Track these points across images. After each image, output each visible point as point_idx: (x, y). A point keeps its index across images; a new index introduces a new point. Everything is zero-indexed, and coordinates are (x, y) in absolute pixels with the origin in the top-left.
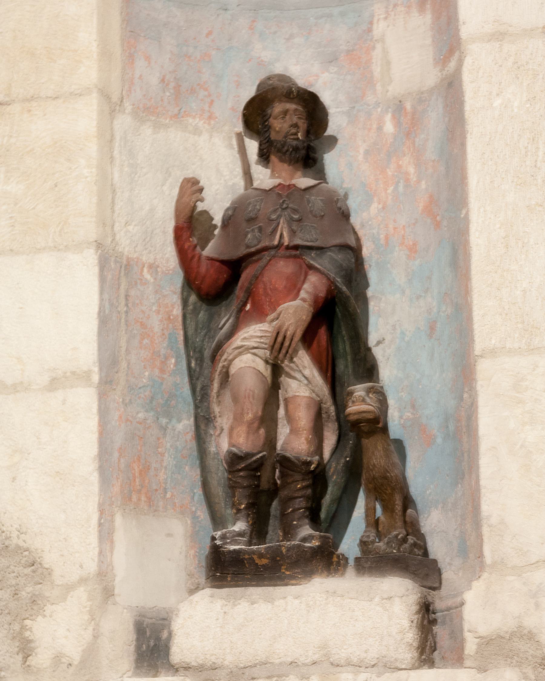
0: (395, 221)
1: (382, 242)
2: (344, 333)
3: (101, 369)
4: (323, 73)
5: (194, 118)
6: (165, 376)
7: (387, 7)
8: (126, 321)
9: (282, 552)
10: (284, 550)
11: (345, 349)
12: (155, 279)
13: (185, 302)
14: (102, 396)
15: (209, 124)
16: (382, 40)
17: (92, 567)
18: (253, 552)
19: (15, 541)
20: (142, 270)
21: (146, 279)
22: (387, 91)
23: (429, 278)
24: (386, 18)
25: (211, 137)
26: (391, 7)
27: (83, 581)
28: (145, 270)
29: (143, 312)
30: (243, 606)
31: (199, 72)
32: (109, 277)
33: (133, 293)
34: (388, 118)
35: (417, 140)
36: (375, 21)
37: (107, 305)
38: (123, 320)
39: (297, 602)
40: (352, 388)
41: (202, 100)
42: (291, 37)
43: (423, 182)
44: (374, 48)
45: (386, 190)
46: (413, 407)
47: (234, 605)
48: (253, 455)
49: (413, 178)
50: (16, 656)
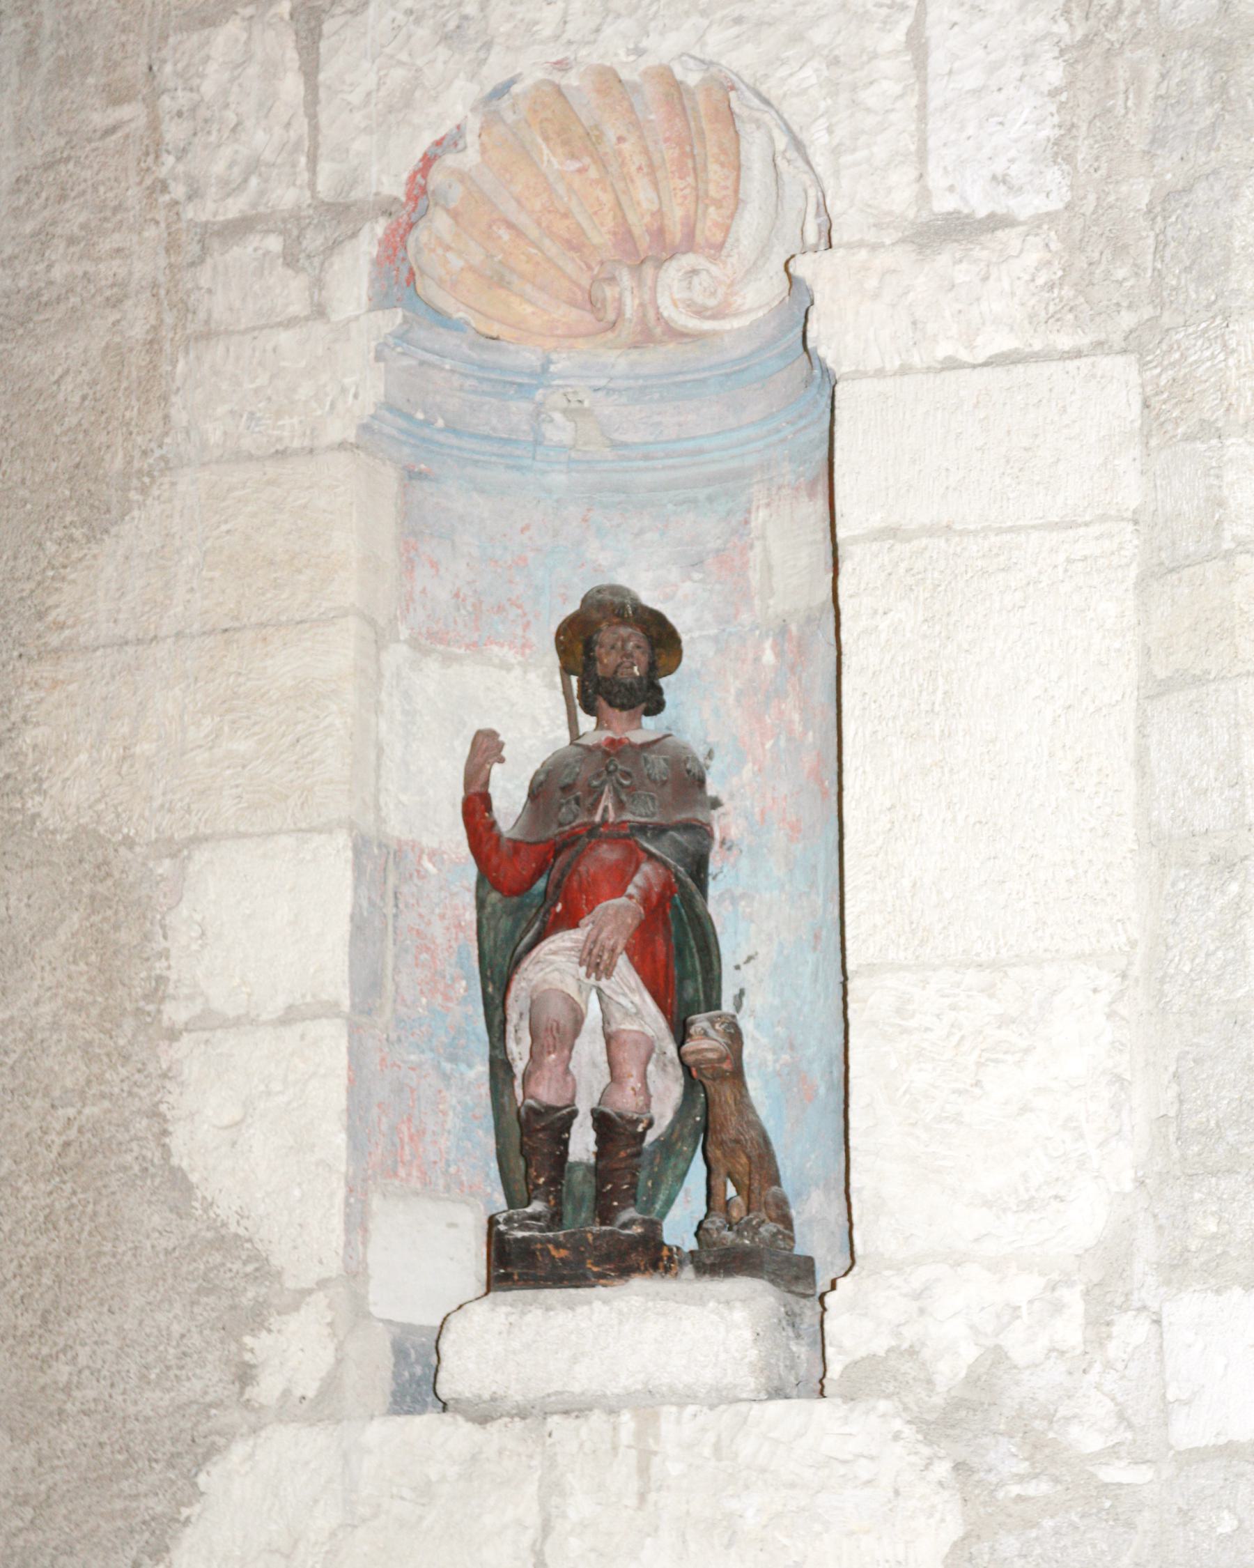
0: (774, 789)
1: (757, 817)
2: (692, 943)
3: (353, 993)
4: (683, 581)
5: (502, 646)
6: (450, 1005)
7: (769, 489)
8: (395, 928)
9: (587, 1240)
10: (590, 1237)
11: (693, 966)
12: (440, 870)
13: (481, 904)
14: (354, 1030)
15: (523, 654)
16: (763, 537)
17: (334, 1267)
18: (549, 1240)
19: (233, 1228)
20: (420, 858)
21: (426, 871)
23: (814, 867)
24: (768, 505)
25: (525, 672)
27: (322, 1284)
28: (425, 858)
29: (421, 916)
30: (535, 1316)
31: (511, 582)
32: (370, 867)
33: (405, 889)
34: (768, 644)
35: (804, 675)
36: (754, 509)
37: (365, 903)
38: (390, 928)
39: (606, 1309)
40: (693, 1017)
41: (513, 621)
43: (811, 734)
44: (752, 547)
45: (763, 745)
46: (792, 1047)
47: (523, 1313)
48: (559, 1109)
49: (798, 728)
50: (231, 1386)
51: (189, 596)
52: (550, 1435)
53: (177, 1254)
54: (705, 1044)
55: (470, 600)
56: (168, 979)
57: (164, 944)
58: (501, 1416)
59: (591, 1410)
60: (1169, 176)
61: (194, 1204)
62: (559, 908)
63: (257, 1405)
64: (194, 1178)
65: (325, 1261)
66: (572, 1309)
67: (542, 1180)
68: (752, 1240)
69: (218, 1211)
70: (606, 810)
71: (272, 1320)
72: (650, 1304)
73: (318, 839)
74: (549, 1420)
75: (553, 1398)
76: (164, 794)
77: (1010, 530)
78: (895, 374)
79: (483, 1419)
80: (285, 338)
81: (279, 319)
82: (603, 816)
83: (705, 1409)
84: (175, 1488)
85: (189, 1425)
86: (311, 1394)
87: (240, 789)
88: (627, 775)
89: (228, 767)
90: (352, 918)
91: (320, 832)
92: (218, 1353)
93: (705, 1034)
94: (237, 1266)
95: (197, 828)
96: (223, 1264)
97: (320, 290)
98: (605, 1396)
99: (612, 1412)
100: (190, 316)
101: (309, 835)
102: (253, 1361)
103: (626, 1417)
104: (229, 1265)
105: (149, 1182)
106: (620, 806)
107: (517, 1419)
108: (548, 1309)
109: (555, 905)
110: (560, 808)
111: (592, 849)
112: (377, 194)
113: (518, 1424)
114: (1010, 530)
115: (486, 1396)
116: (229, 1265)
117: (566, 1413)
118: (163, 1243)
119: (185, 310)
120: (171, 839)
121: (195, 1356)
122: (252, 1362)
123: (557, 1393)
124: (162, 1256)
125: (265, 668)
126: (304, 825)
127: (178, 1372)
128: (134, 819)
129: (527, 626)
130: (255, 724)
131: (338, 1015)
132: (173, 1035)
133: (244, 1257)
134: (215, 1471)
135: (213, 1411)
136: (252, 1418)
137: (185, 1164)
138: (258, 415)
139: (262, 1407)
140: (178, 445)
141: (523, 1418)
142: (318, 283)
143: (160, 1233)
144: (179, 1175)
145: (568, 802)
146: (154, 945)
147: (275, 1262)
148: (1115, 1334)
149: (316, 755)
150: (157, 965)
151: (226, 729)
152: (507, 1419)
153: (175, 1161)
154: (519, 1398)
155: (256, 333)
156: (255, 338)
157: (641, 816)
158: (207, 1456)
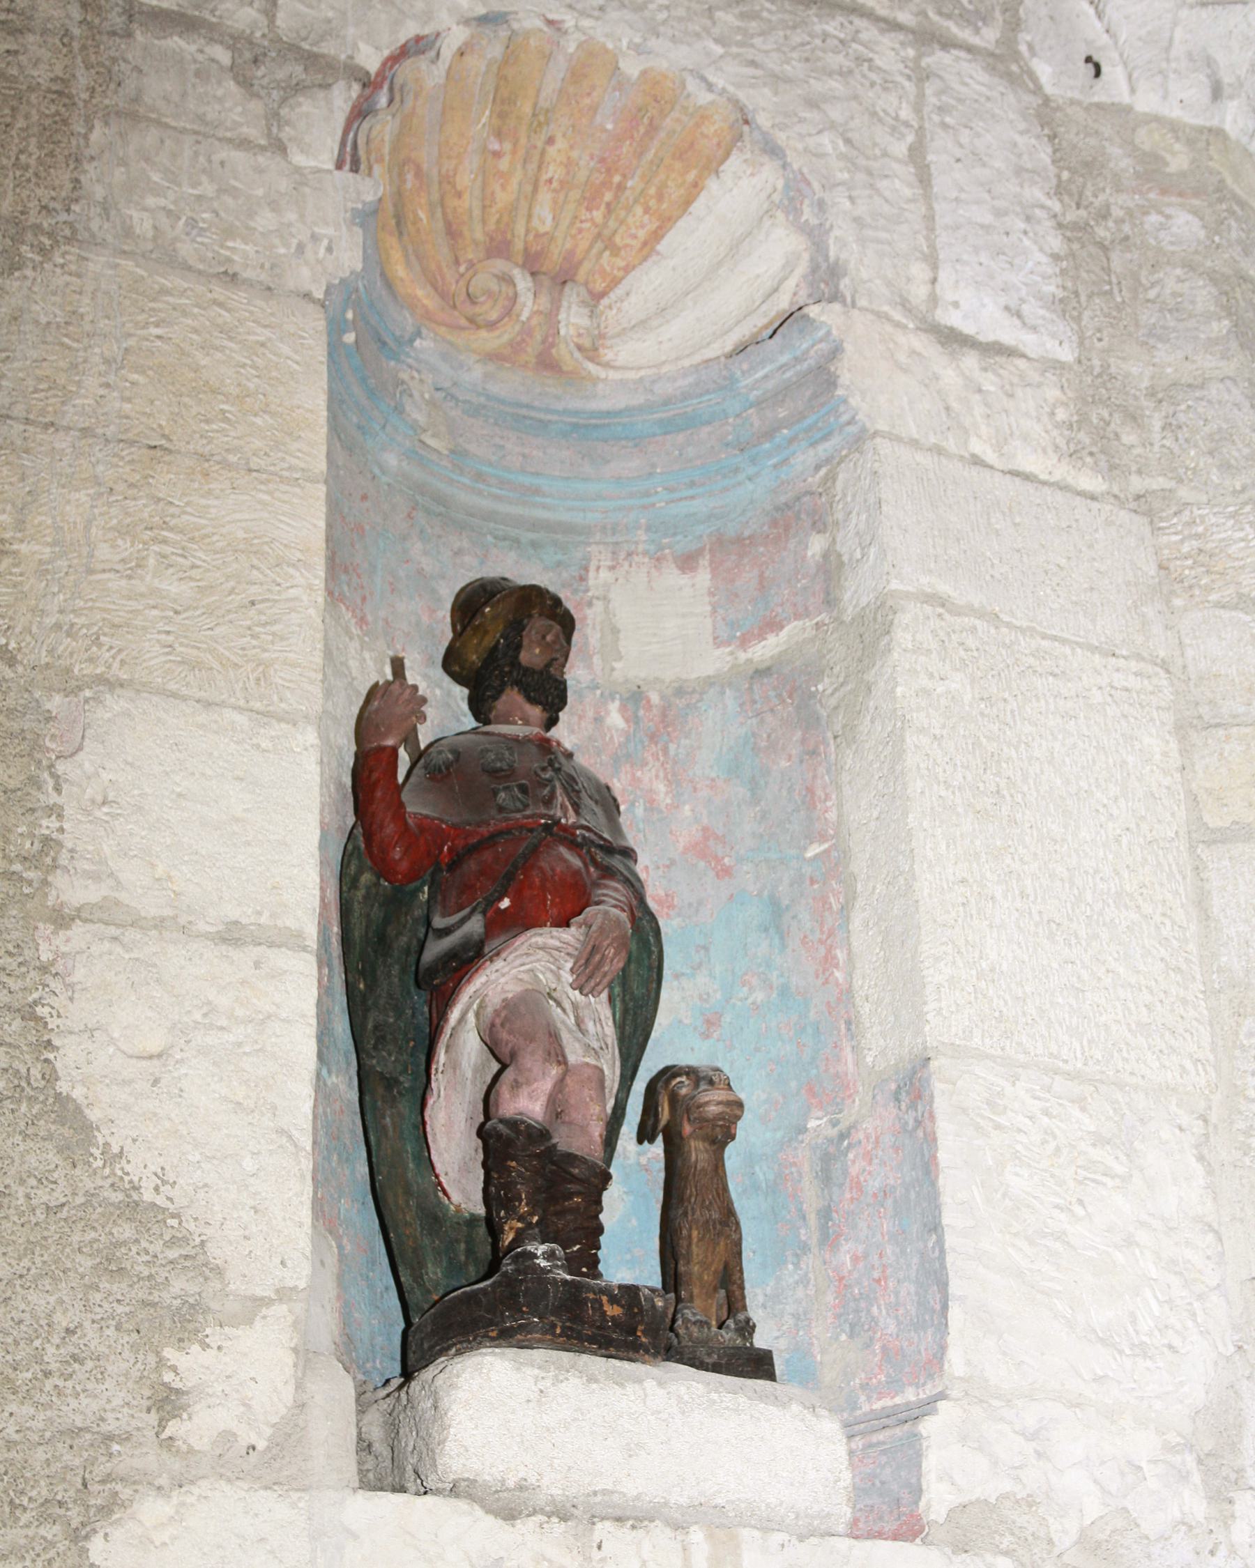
19: (148, 1196)
22: (613, 669)
26: (622, 555)
27: (283, 1294)
30: (573, 1386)
39: (661, 1392)
42: (458, 553)
47: (557, 1381)
50: (144, 1415)
51: (102, 392)
52: (599, 1547)
53: (64, 1213)
56: (60, 844)
57: (54, 798)
58: (534, 1513)
59: (652, 1521)
60: (1169, 370)
61: (93, 1150)
62: (505, 903)
63: (184, 1448)
64: (93, 1115)
65: (289, 1264)
66: (622, 1385)
67: (536, 1219)
69: (128, 1168)
71: (208, 1331)
72: (714, 1396)
73: (278, 728)
74: (599, 1526)
75: (599, 1498)
76: (61, 612)
77: (1055, 638)
78: (930, 449)
79: (509, 1515)
80: (238, 157)
81: (228, 135)
83: (794, 1540)
84: (52, 1553)
85: (77, 1462)
86: (261, 1445)
87: (171, 638)
89: (154, 607)
91: (280, 720)
92: (124, 1365)
94: (157, 1247)
95: (109, 667)
96: (137, 1241)
97: (279, 127)
98: (666, 1504)
99: (678, 1526)
100: (112, 86)
101: (265, 720)
102: (177, 1385)
103: (697, 1535)
104: (144, 1244)
105: (24, 1107)
107: (555, 1519)
109: (500, 899)
111: (548, 846)
112: (351, 57)
113: (557, 1527)
114: (1055, 638)
115: (511, 1483)
116: (144, 1244)
117: (619, 1519)
118: (42, 1196)
119: (108, 76)
120: (68, 670)
121: (90, 1364)
122: (175, 1385)
123: (605, 1492)
124: (40, 1216)
125: (208, 506)
126: (257, 705)
127: (61, 1383)
128: (17, 630)
130: (194, 567)
131: (305, 949)
132: (62, 919)
133: (167, 1237)
134: (117, 1534)
135: (116, 1447)
136: (176, 1465)
137: (78, 1093)
138: (201, 225)
139: (191, 1451)
140: (89, 219)
141: (564, 1518)
142: (274, 117)
143: (40, 1181)
144: (71, 1106)
146: (41, 797)
147: (216, 1253)
148: (1237, 1514)
149: (276, 628)
150: (45, 823)
151: (152, 561)
152: (541, 1518)
153: (63, 1087)
154: (556, 1491)
155: (200, 138)
156: (198, 142)
158: (106, 1510)
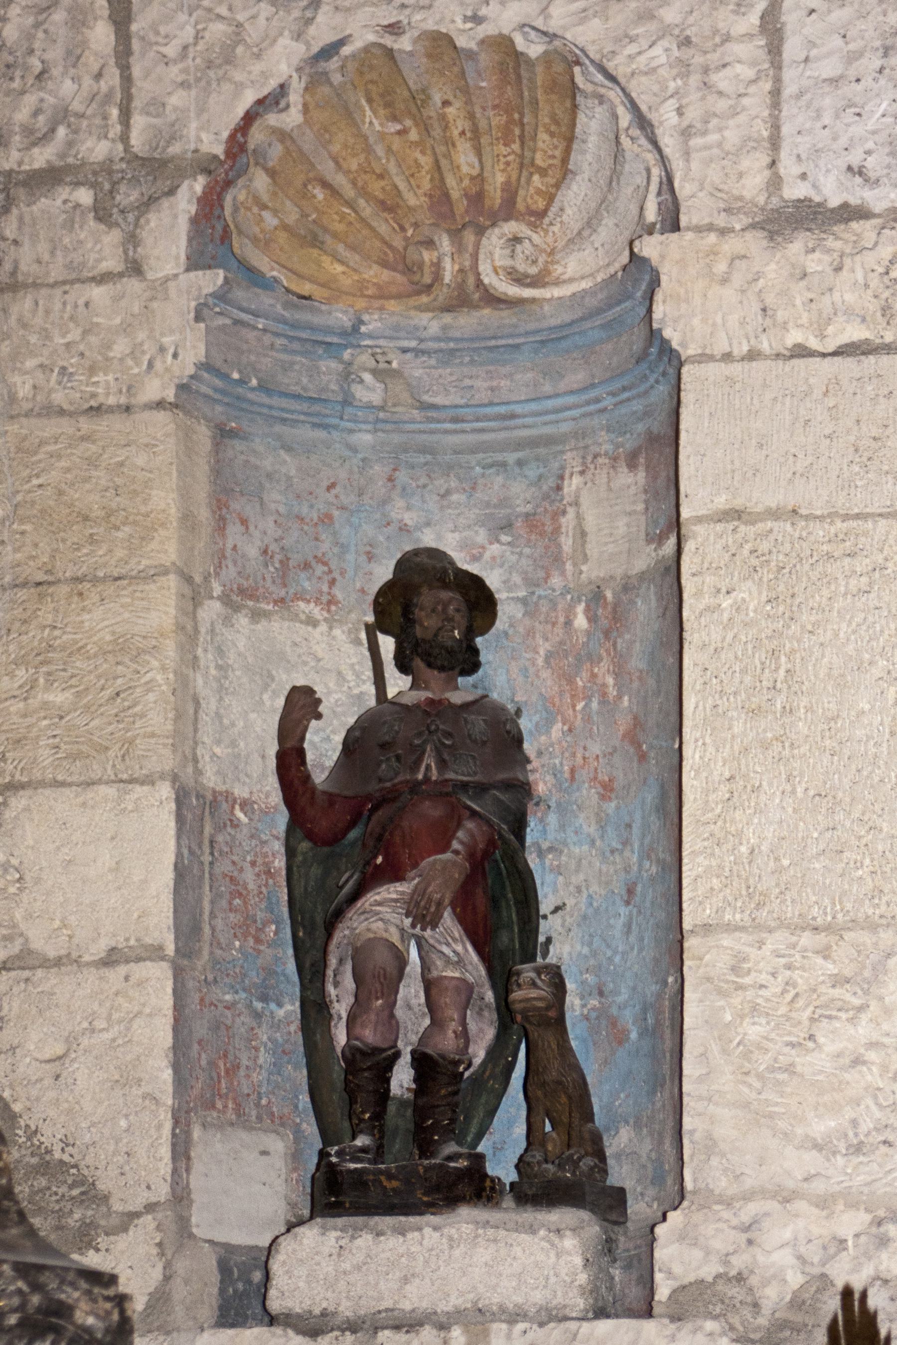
2: (510, 895)
4: (491, 543)
5: (309, 602)
8: (211, 874)
9: (418, 1172)
10: (421, 1170)
11: (510, 917)
12: (250, 819)
14: (178, 974)
15: (329, 611)
16: (576, 504)
17: (163, 1192)
18: (381, 1172)
19: (57, 1155)
20: (233, 807)
21: (238, 819)
22: (581, 572)
23: (629, 826)
24: (582, 473)
25: (331, 628)
27: (150, 1208)
28: (237, 807)
29: (234, 863)
30: (365, 1240)
31: (317, 539)
32: (190, 816)
33: (220, 838)
34: (580, 608)
35: (619, 641)
36: (567, 476)
37: (185, 852)
38: (207, 875)
39: (436, 1235)
41: (319, 578)
43: (626, 698)
44: (564, 512)
45: (574, 706)
47: (353, 1238)
48: (385, 1050)
49: (612, 692)
54: (534, 993)
55: (278, 557)
58: (332, 1330)
59: (421, 1325)
61: (17, 1132)
65: (153, 1187)
66: (404, 1235)
68: (574, 1173)
69: (42, 1139)
70: (428, 767)
71: (99, 1240)
72: (480, 1231)
74: (380, 1334)
75: (384, 1314)
79: (314, 1333)
80: (98, 293)
81: (90, 275)
82: (425, 775)
88: (449, 735)
90: (176, 865)
93: (534, 984)
94: (63, 1190)
96: (49, 1188)
97: (135, 247)
98: (435, 1313)
99: (443, 1327)
104: (54, 1189)
106: (442, 764)
107: (348, 1333)
108: (378, 1234)
110: (379, 765)
115: (317, 1311)
116: (54, 1189)
117: (397, 1328)
123: (387, 1310)
129: (333, 582)
133: (70, 1182)
138: (71, 370)
141: (354, 1331)
142: (132, 239)
145: (388, 759)
154: (348, 1314)
155: (67, 287)
156: (65, 293)
157: (464, 775)
